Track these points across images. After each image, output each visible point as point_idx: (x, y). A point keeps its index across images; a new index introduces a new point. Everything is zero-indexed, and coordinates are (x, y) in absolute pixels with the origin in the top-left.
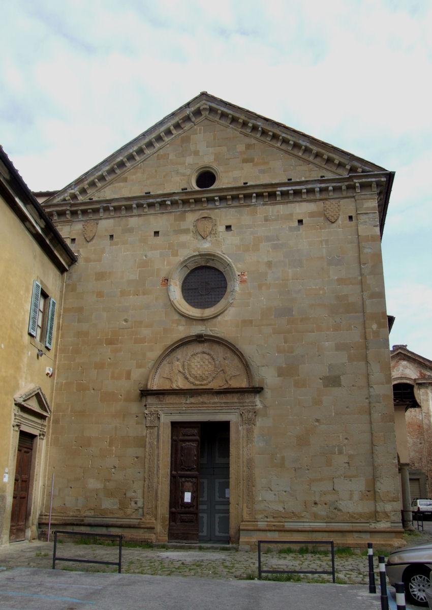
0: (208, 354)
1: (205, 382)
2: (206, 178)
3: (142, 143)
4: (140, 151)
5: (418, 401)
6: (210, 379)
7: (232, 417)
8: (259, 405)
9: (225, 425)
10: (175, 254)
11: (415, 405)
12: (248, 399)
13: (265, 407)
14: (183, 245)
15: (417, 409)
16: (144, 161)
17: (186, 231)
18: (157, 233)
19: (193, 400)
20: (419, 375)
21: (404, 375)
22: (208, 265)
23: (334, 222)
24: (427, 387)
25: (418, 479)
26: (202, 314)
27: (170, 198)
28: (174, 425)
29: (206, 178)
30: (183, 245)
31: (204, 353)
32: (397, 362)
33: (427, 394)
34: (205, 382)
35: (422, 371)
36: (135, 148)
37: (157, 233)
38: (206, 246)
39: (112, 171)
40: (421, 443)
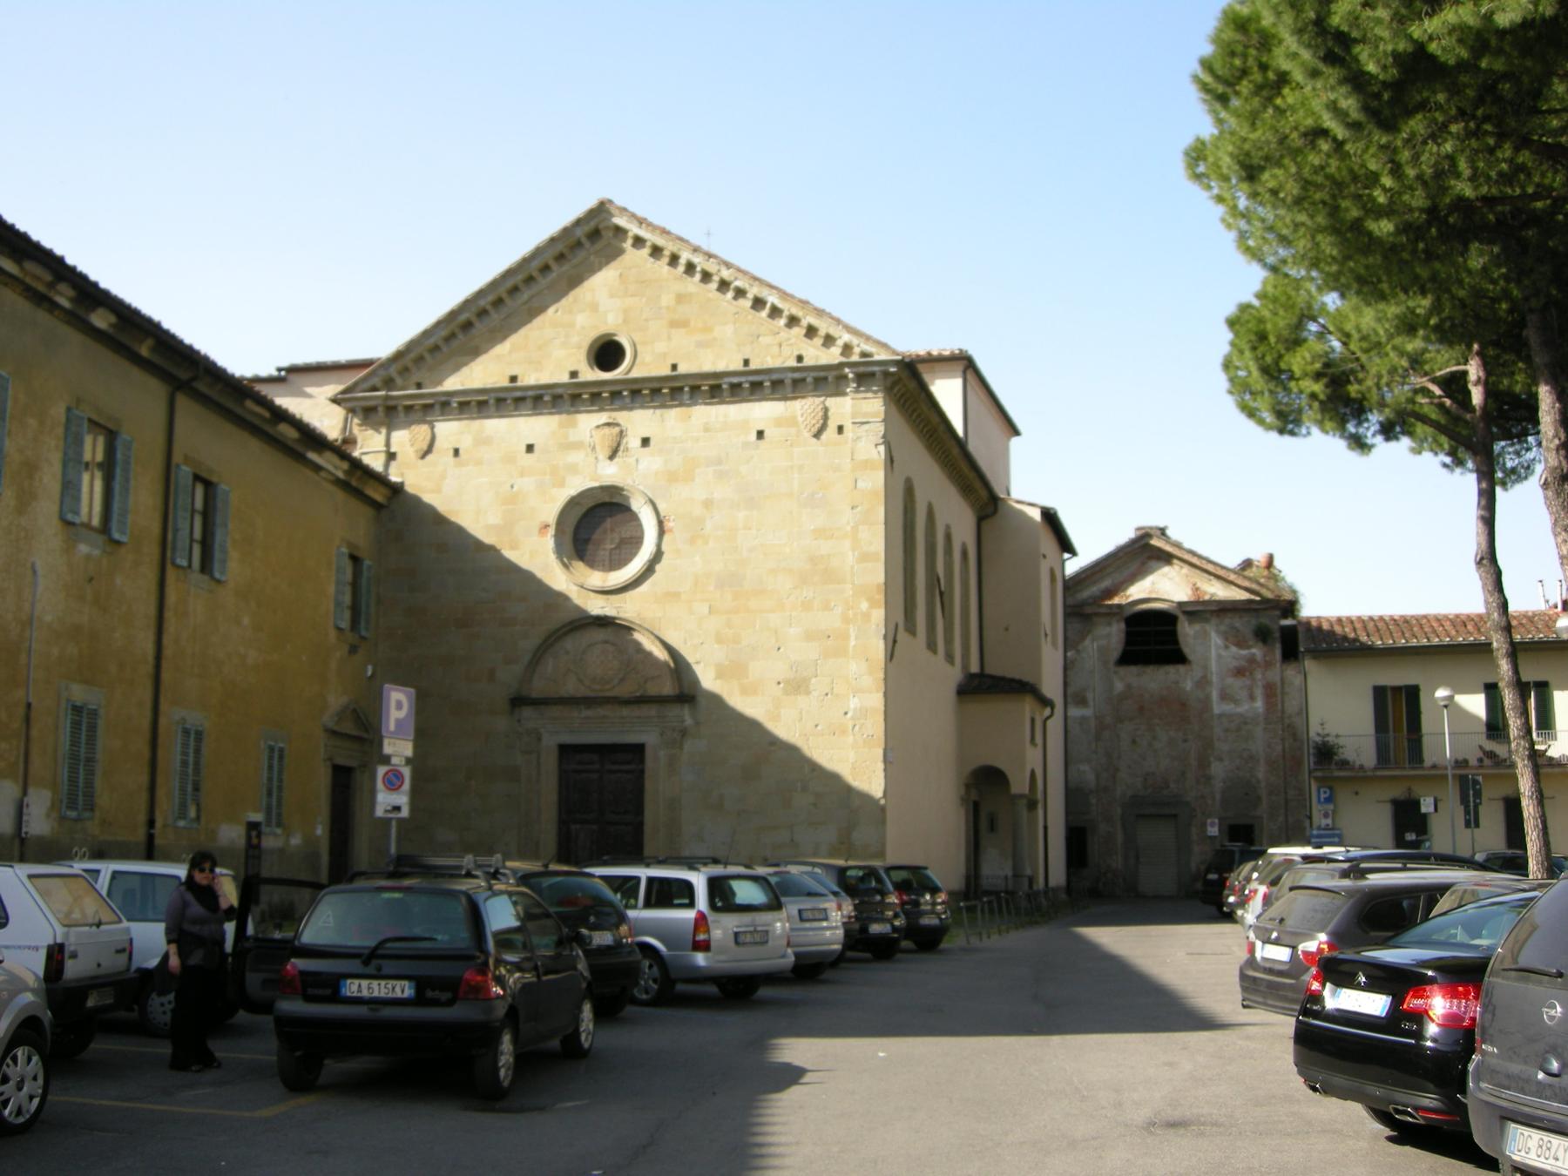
0: (613, 644)
1: (607, 687)
2: (607, 353)
3: (502, 291)
4: (498, 302)
5: (1186, 650)
6: (616, 681)
7: (649, 737)
8: (689, 721)
9: (638, 750)
10: (562, 484)
11: (1178, 657)
12: (673, 711)
13: (697, 723)
14: (573, 469)
15: (1182, 668)
16: (505, 318)
17: (576, 446)
18: (530, 448)
19: (589, 713)
20: (1190, 592)
21: (1157, 593)
22: (615, 500)
23: (867, 375)
24: (1207, 621)
25: (1175, 816)
26: (604, 581)
27: (549, 391)
28: (565, 750)
29: (607, 353)
30: (573, 469)
31: (606, 642)
32: (1143, 564)
33: (1206, 634)
34: (607, 687)
35: (1199, 585)
36: (491, 298)
37: (530, 448)
38: (608, 473)
39: (451, 337)
40: (1185, 741)
